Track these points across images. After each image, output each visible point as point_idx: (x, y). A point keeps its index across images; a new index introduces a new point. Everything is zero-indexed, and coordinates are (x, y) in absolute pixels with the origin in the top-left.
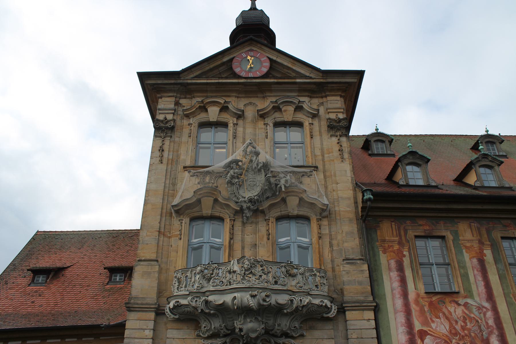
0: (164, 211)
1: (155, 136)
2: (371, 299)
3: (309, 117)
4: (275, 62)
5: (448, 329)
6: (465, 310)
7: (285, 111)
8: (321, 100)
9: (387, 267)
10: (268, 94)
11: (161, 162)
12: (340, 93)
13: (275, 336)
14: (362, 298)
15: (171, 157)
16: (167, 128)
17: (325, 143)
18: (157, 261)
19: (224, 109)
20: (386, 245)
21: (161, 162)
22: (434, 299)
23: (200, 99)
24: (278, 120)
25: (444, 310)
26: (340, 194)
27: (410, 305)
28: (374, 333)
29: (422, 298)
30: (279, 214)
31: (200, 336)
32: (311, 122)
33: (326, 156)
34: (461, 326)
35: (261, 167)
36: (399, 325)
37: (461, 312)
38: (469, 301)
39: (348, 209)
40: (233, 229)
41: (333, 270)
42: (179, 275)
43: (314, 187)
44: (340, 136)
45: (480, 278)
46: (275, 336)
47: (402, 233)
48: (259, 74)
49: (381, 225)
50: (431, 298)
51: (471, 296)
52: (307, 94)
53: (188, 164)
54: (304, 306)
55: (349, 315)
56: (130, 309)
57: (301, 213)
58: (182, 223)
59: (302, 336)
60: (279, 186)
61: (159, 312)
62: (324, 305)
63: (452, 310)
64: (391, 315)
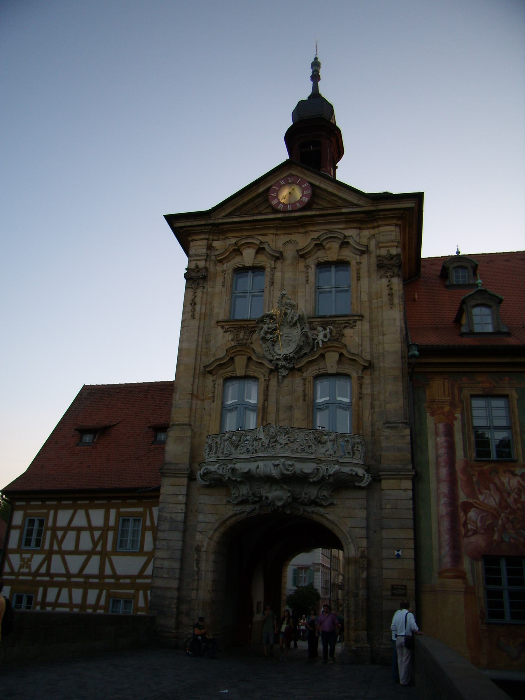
0: (197, 372)
1: (187, 288)
2: (410, 467)
3: (357, 254)
4: (319, 187)
5: (497, 502)
6: (521, 481)
7: (329, 249)
8: (372, 232)
10: (310, 229)
11: (193, 317)
12: (395, 222)
13: (303, 504)
15: (203, 311)
16: (199, 278)
18: (190, 425)
19: (260, 250)
21: (193, 317)
22: (485, 468)
23: (233, 241)
24: (322, 260)
25: (497, 481)
28: (410, 504)
31: (230, 502)
32: (358, 261)
33: (375, 301)
34: (515, 500)
35: (296, 321)
37: (516, 483)
40: (267, 390)
42: (210, 441)
43: (357, 339)
46: (303, 504)
47: (456, 391)
53: (222, 317)
54: (330, 476)
55: (385, 484)
56: (163, 475)
57: (340, 371)
58: (215, 384)
59: (332, 504)
60: (316, 341)
61: (191, 478)
62: (354, 473)
63: (505, 481)
64: (433, 485)
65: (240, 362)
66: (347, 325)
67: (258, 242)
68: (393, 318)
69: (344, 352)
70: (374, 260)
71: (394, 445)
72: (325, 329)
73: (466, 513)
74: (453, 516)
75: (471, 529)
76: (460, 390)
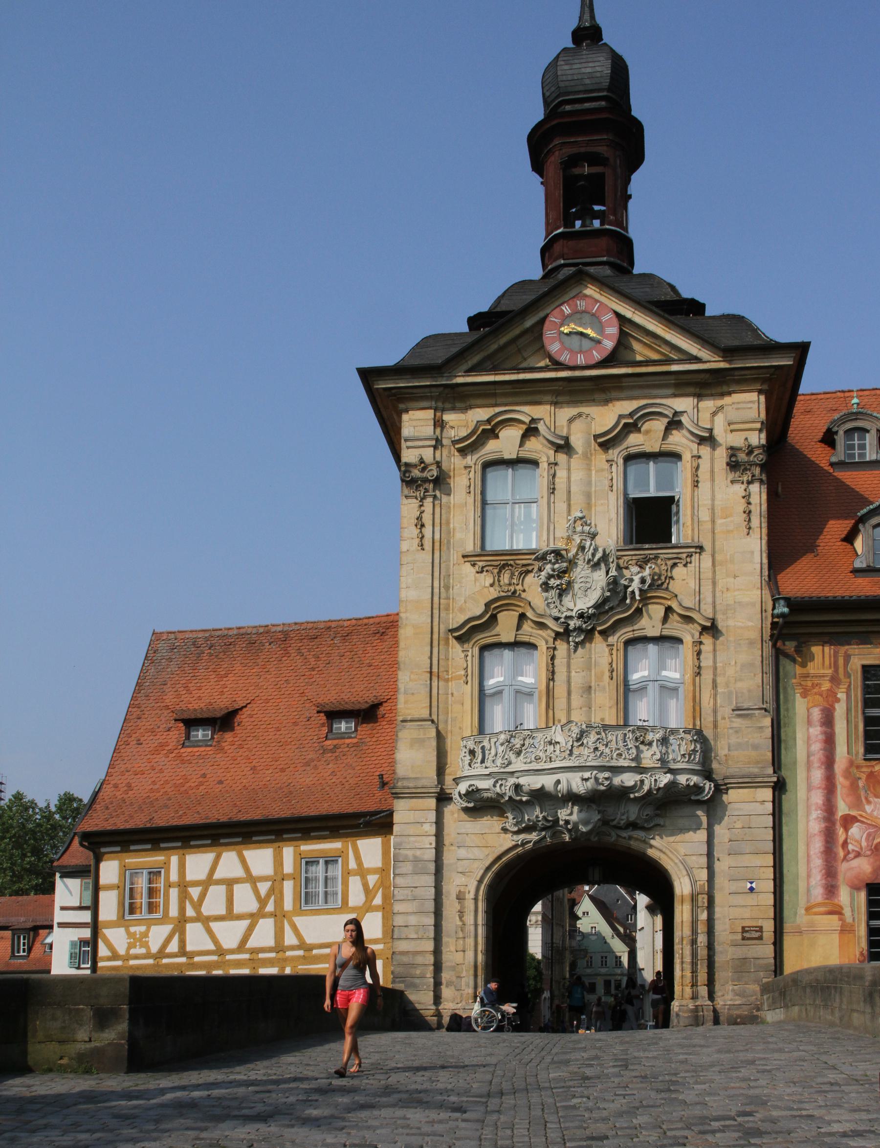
2: (770, 771)
3: (693, 441)
4: (630, 321)
7: (647, 432)
8: (720, 402)
9: (806, 720)
10: (614, 394)
14: (756, 770)
17: (718, 496)
20: (809, 684)
27: (834, 778)
29: (858, 767)
30: (630, 635)
32: (695, 453)
33: (719, 522)
36: (813, 808)
39: (750, 624)
41: (715, 726)
43: (692, 584)
44: (749, 483)
46: (620, 828)
48: (597, 356)
49: (804, 649)
50: (873, 766)
52: (692, 390)
57: (666, 633)
66: (677, 561)
69: (674, 605)
73: (847, 830)
74: (829, 835)
75: (853, 851)
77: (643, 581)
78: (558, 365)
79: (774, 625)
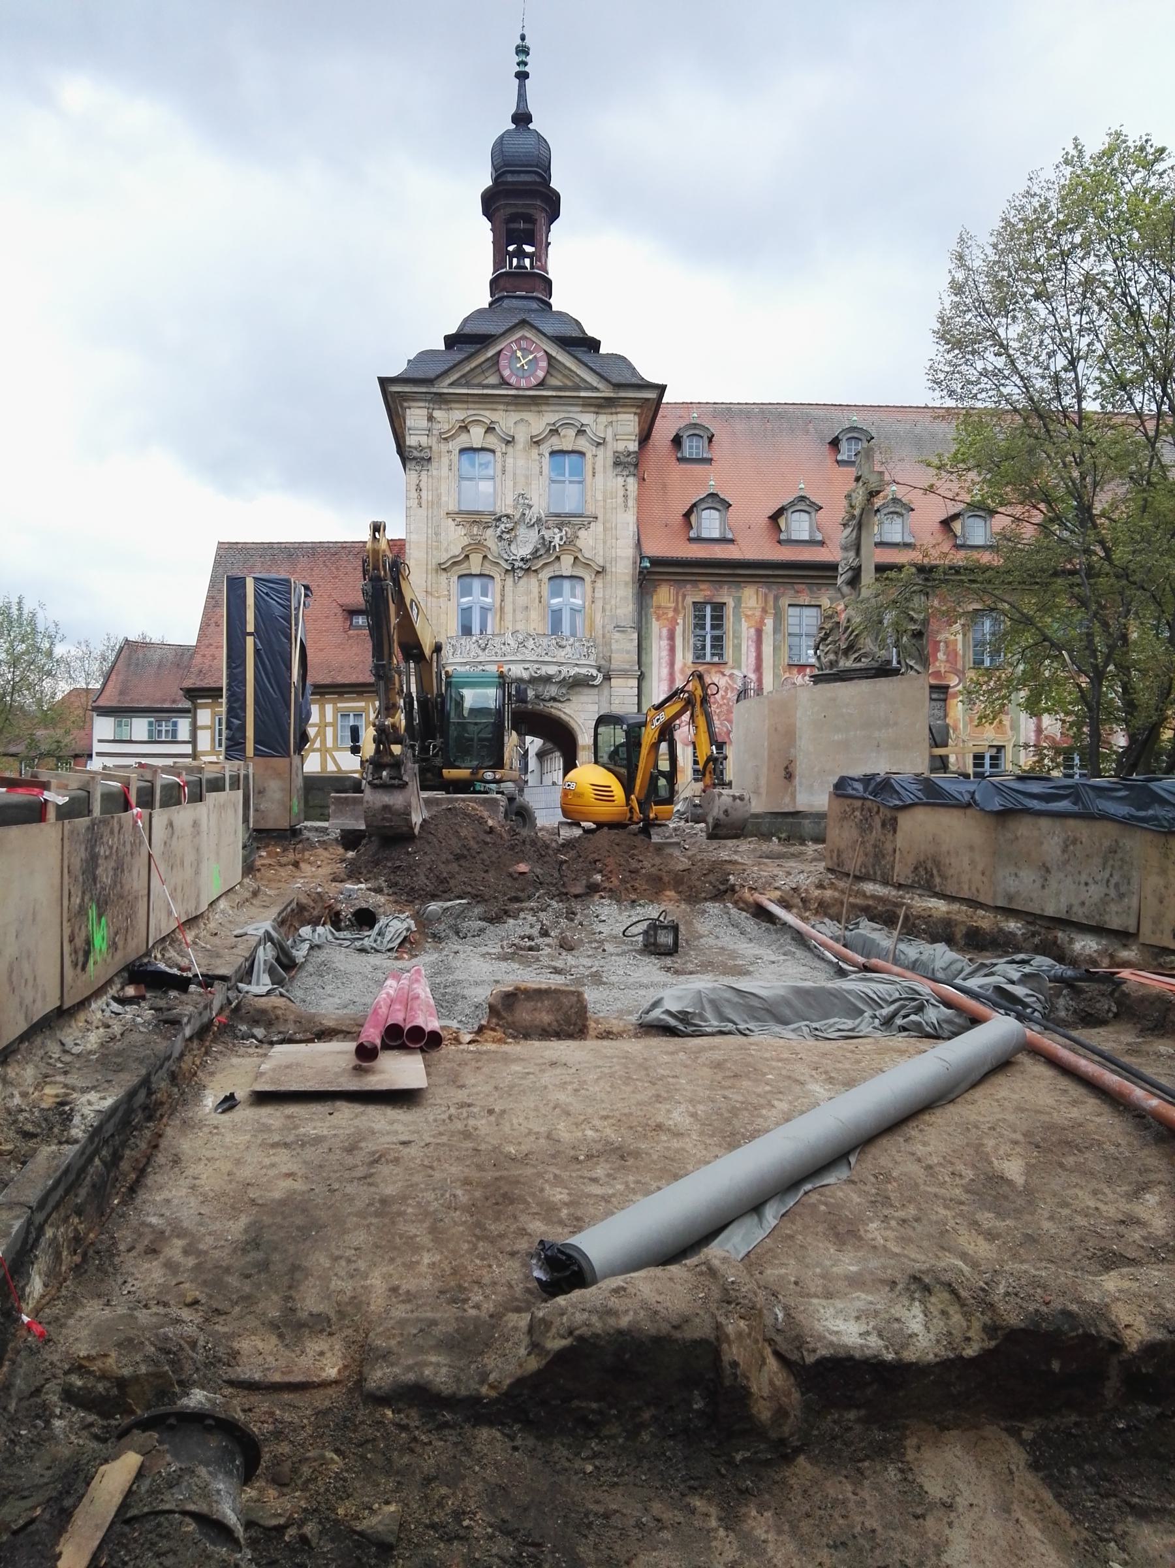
7: (565, 436)
10: (544, 408)
13: (543, 700)
16: (423, 459)
19: (490, 430)
24: (556, 448)
26: (620, 553)
38: (736, 672)
43: (591, 542)
45: (753, 649)
46: (543, 700)
47: (680, 598)
48: (534, 382)
51: (739, 667)
52: (593, 409)
53: (453, 507)
64: (655, 684)
65: (476, 559)
67: (488, 422)
68: (627, 521)
70: (610, 454)
71: (623, 649)
72: (561, 530)
76: (684, 596)
77: (561, 539)
78: (504, 383)
79: (640, 573)
